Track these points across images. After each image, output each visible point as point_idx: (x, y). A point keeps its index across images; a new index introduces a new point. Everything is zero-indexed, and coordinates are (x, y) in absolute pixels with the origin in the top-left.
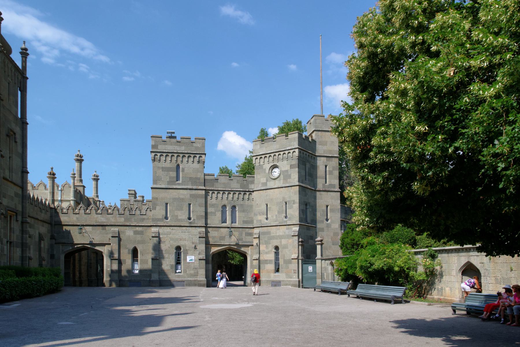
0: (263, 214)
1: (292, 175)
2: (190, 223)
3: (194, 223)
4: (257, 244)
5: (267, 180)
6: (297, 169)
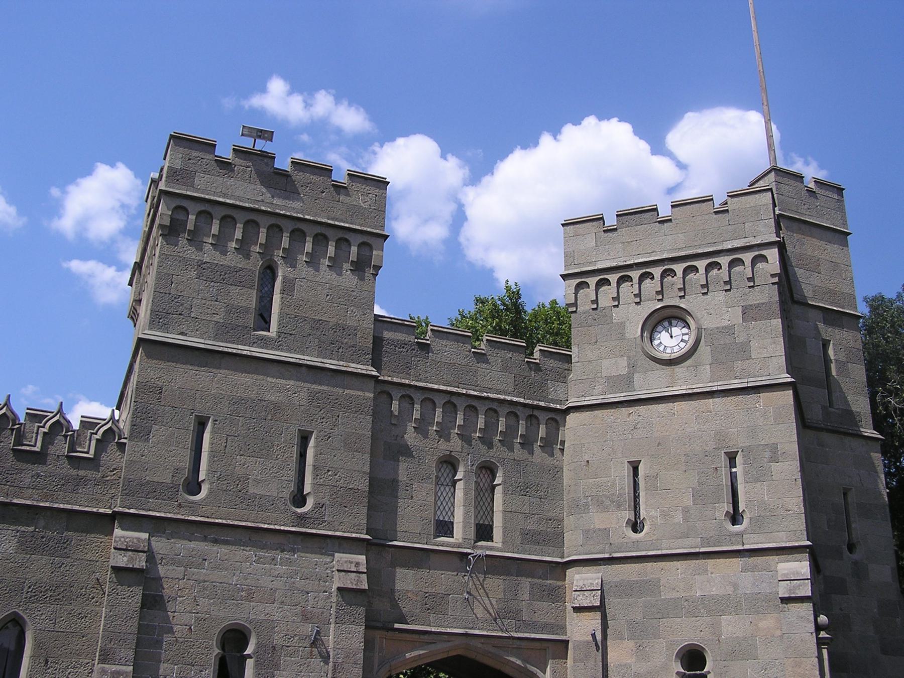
0: (619, 506)
1: (754, 344)
2: (302, 519)
4: (594, 635)
5: (633, 367)
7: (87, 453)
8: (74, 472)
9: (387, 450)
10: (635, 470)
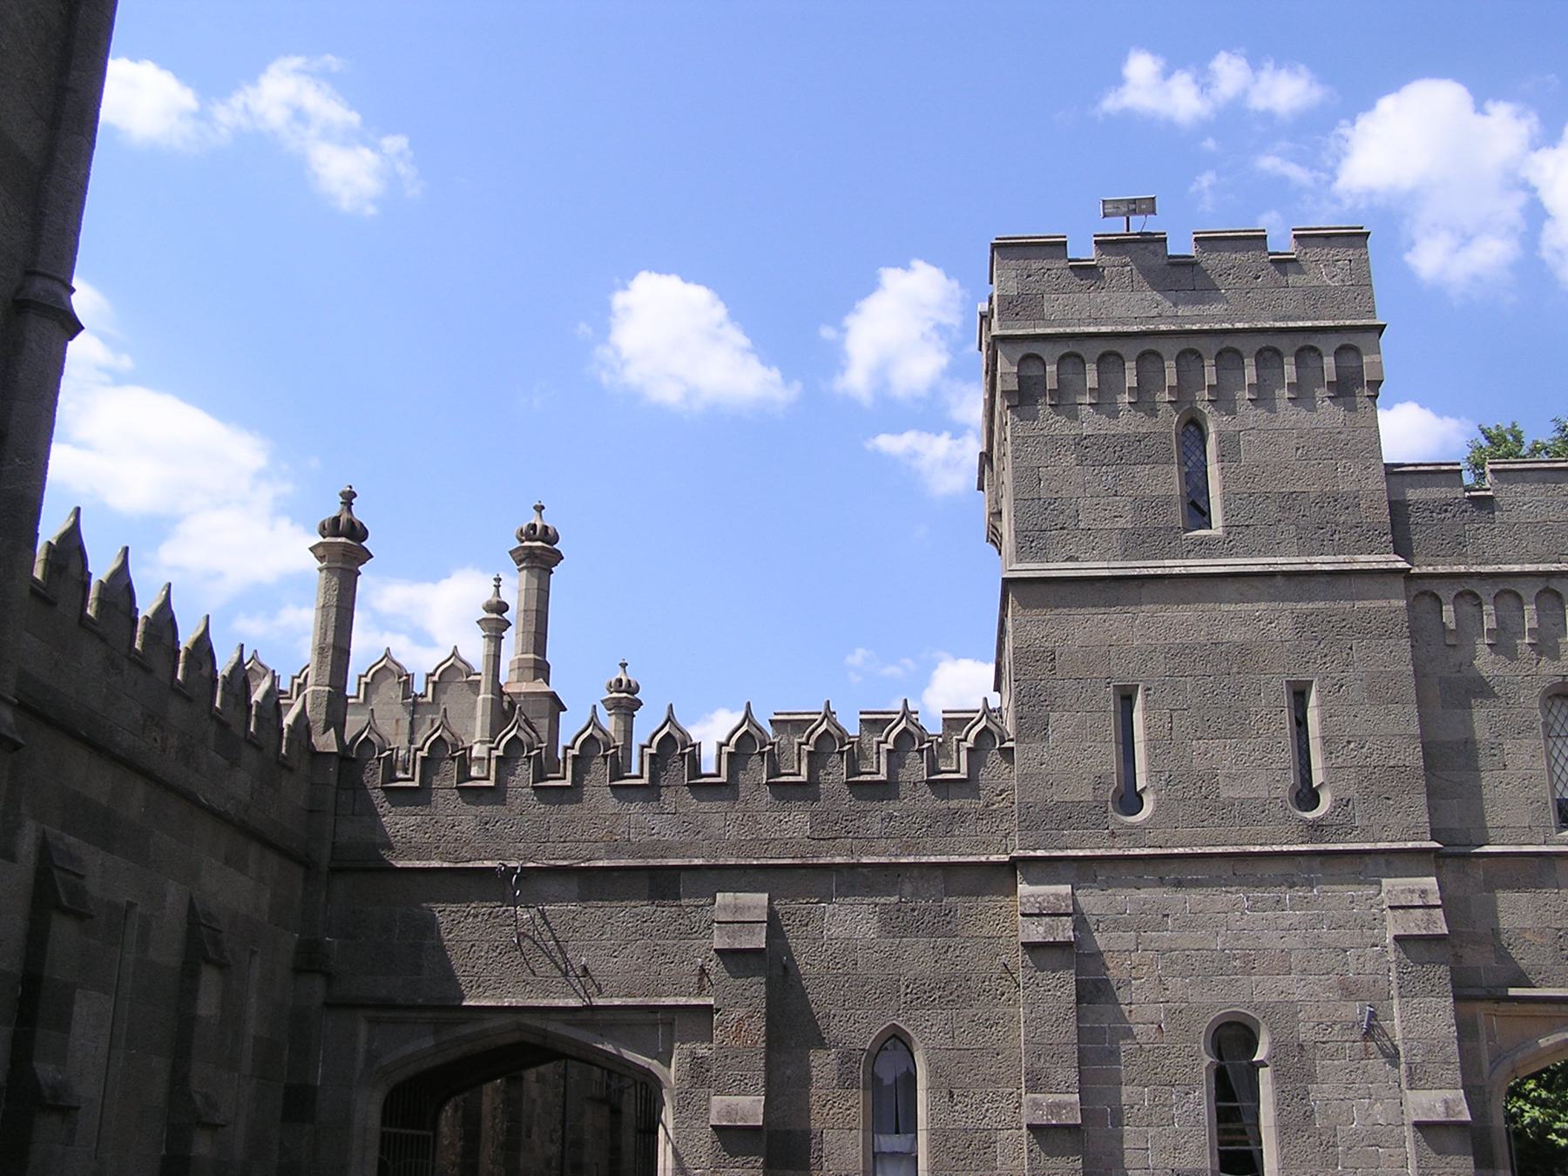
2: (1316, 829)
3: (1346, 829)
7: (958, 771)
8: (942, 805)
9: (1445, 691)
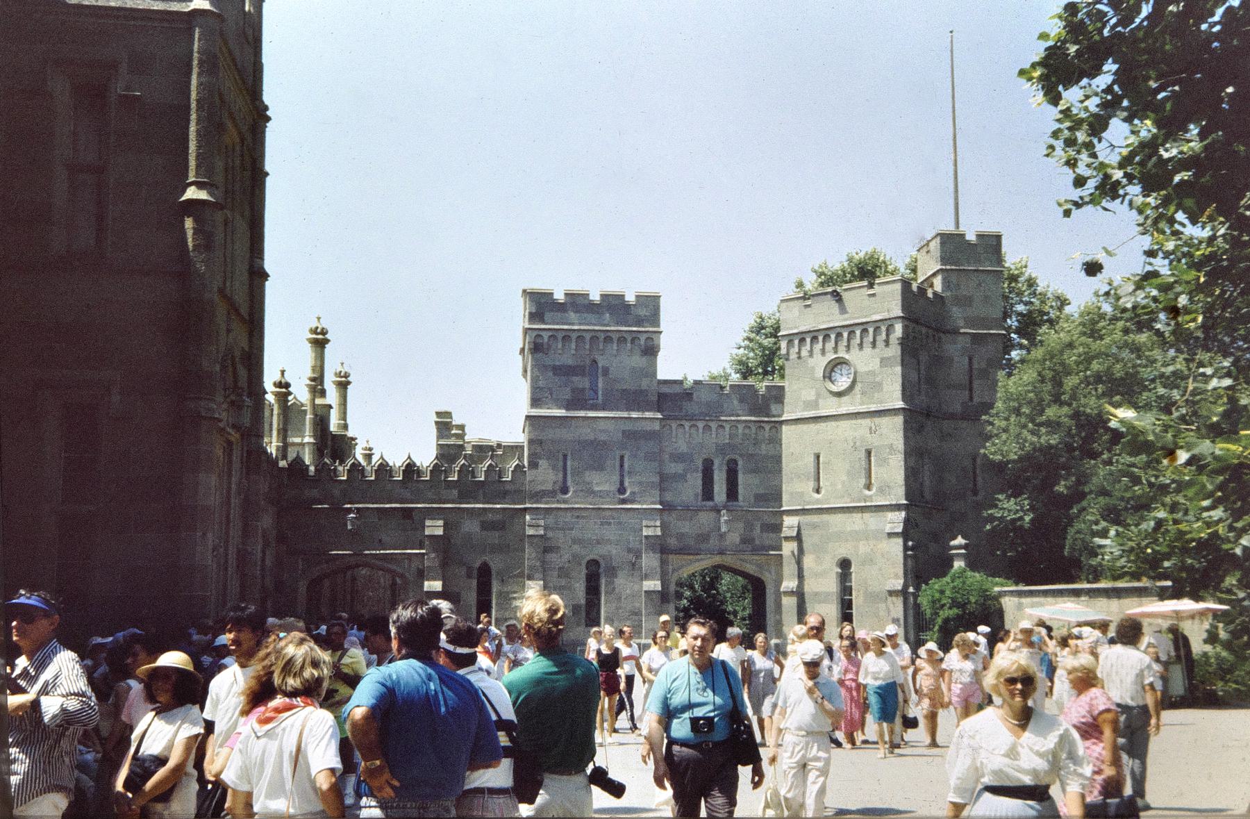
5: (818, 395)
6: (898, 369)
10: (818, 457)
